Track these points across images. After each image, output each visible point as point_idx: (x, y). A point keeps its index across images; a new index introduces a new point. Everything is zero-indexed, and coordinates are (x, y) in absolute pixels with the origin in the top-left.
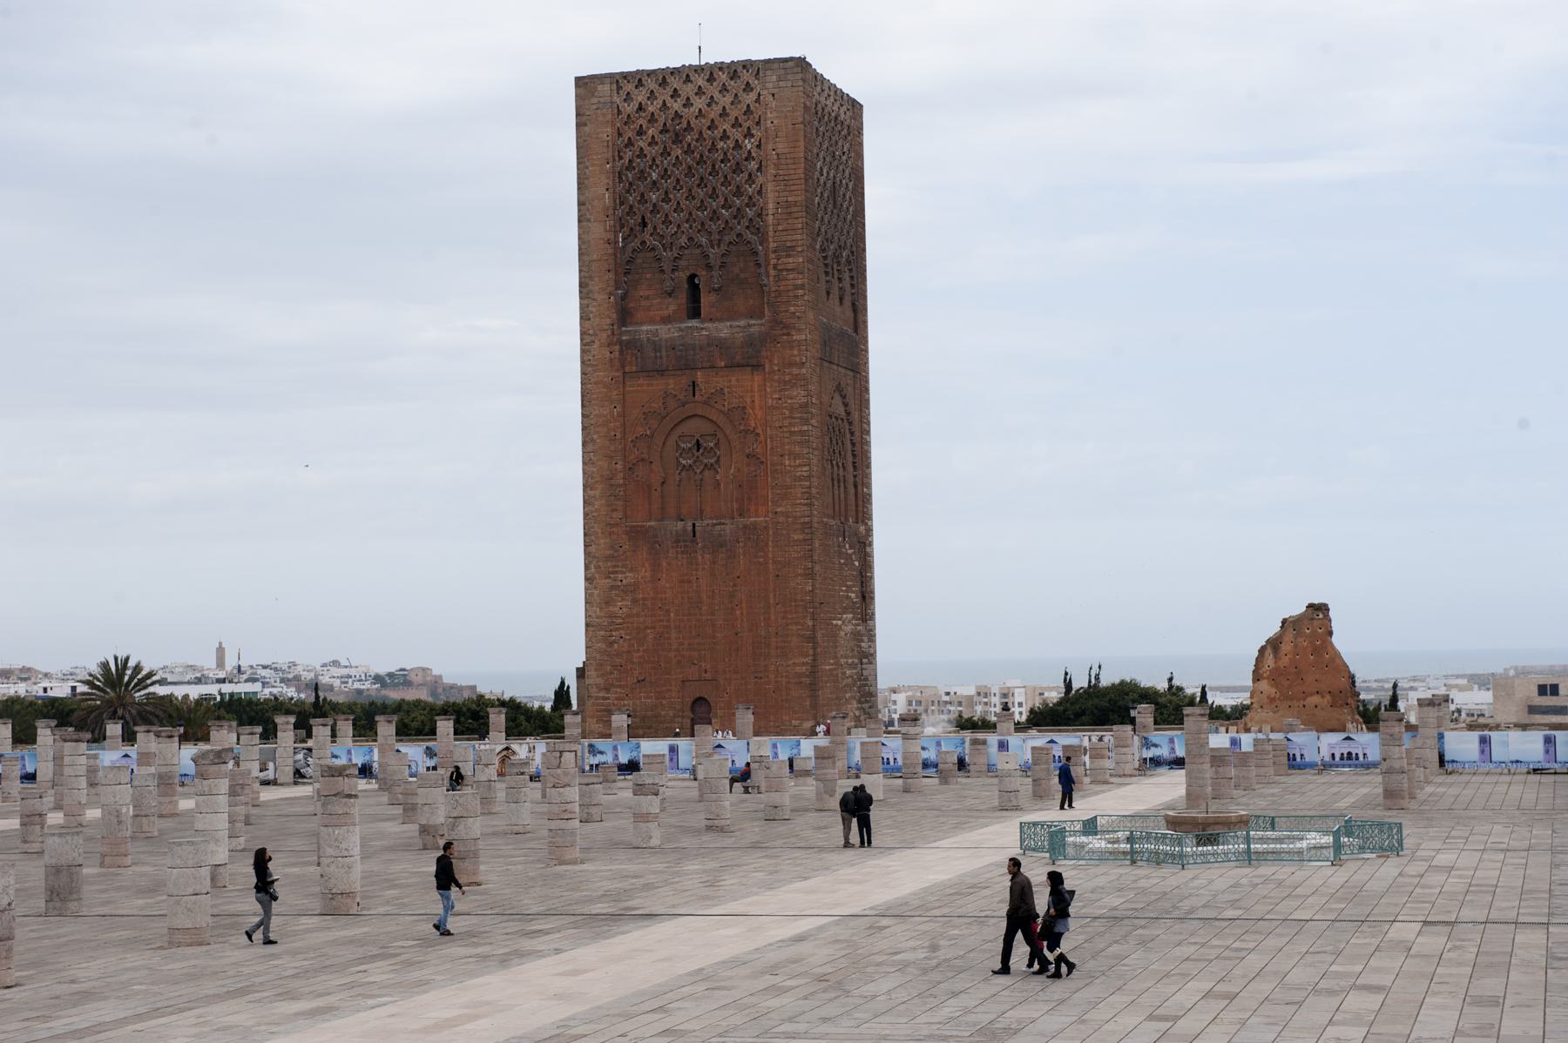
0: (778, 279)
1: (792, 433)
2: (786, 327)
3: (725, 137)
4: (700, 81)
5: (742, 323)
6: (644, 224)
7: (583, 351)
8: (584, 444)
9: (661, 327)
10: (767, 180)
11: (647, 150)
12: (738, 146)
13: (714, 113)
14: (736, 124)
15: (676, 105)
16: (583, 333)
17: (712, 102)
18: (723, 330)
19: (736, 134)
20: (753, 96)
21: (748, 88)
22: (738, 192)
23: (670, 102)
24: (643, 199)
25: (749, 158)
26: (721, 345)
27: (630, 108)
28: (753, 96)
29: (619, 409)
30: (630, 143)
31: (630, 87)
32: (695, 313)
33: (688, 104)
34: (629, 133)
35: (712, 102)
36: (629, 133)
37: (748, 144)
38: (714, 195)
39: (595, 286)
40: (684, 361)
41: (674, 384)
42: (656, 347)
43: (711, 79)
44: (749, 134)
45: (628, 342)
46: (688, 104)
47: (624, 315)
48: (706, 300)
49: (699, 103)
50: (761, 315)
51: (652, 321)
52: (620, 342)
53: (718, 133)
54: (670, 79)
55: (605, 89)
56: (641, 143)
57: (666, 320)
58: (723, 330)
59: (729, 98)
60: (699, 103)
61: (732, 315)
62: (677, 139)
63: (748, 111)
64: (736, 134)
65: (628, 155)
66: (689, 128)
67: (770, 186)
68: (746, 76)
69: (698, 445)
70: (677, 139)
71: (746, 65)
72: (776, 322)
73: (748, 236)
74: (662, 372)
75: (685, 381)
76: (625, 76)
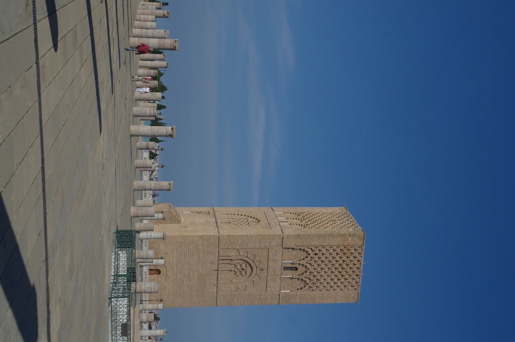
20: (350, 287)
69: (243, 269)
73: (307, 287)
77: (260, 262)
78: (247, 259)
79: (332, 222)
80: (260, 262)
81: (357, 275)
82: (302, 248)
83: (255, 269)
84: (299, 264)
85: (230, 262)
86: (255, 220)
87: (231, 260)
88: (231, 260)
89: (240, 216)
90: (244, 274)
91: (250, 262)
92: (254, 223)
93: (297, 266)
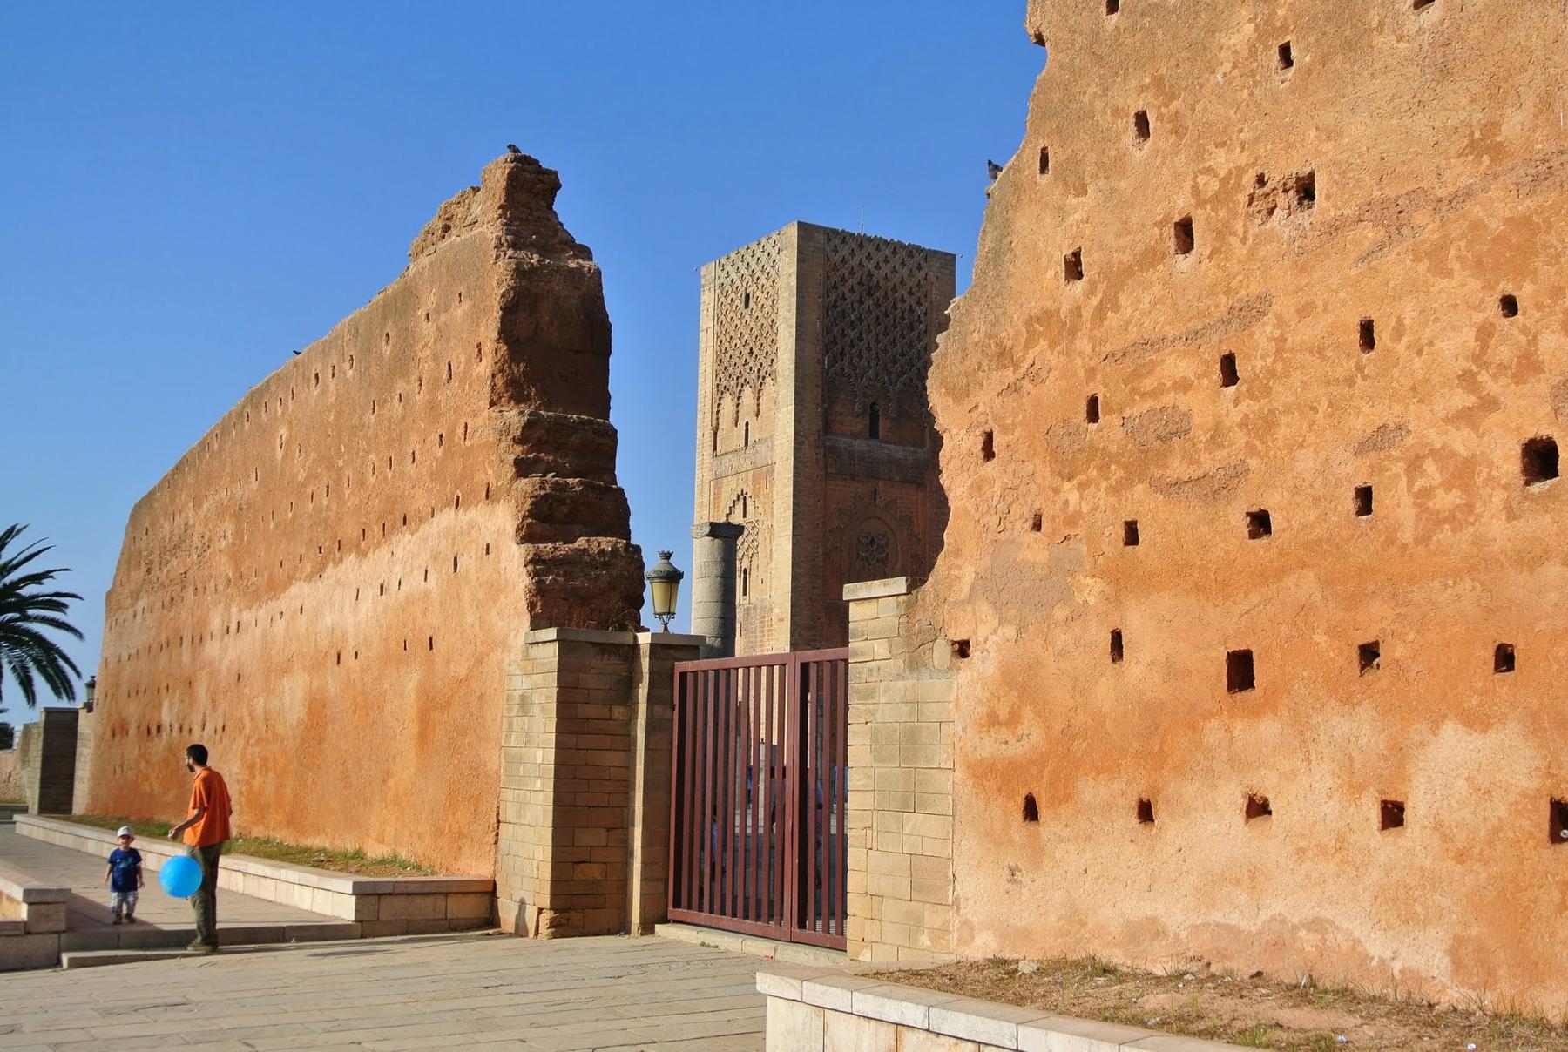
3: (903, 300)
12: (911, 310)
13: (896, 279)
14: (911, 293)
15: (870, 266)
17: (894, 271)
18: (898, 452)
19: (911, 301)
20: (922, 274)
21: (919, 268)
22: (911, 346)
23: (865, 261)
24: (843, 336)
27: (837, 258)
28: (922, 274)
30: (835, 287)
31: (837, 241)
32: (874, 433)
33: (877, 267)
34: (835, 278)
35: (894, 271)
37: (919, 310)
38: (894, 343)
43: (894, 253)
44: (919, 303)
46: (877, 267)
47: (827, 427)
48: (883, 425)
49: (886, 269)
54: (866, 244)
55: (821, 237)
56: (846, 290)
57: (854, 436)
58: (898, 452)
60: (886, 269)
62: (870, 294)
63: (918, 285)
64: (911, 301)
65: (833, 297)
66: (878, 287)
68: (919, 257)
70: (870, 294)
71: (919, 249)
74: (853, 478)
76: (835, 231)
79: (751, 304)
81: (894, 253)
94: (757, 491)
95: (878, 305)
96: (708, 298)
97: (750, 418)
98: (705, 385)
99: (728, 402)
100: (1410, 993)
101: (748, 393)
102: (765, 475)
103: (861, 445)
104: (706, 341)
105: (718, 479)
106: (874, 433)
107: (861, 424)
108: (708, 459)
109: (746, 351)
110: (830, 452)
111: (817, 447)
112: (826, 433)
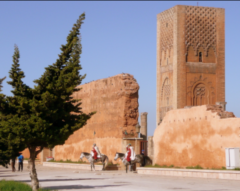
0: (219, 55)
1: (221, 89)
2: (221, 65)
4: (204, 10)
5: (211, 64)
6: (191, 40)
7: (178, 67)
8: (178, 87)
9: (194, 63)
10: (217, 33)
11: (192, 23)
16: (178, 62)
18: (208, 65)
25: (213, 28)
26: (206, 68)
29: (185, 80)
32: (200, 60)
36: (189, 19)
37: (213, 25)
39: (181, 52)
40: (199, 71)
41: (197, 76)
42: (193, 67)
45: (187, 66)
50: (215, 62)
51: (192, 61)
52: (186, 66)
53: (207, 22)
57: (195, 61)
58: (208, 65)
59: (209, 15)
61: (208, 62)
67: (217, 35)
69: (200, 90)
72: (218, 64)
75: (199, 75)
77: (195, 78)
78: (193, 87)
80: (195, 78)
82: (186, 49)
83: (200, 82)
84: (198, 51)
85: (195, 99)
86: (166, 81)
87: (194, 98)
88: (194, 98)
89: (164, 91)
90: (203, 89)
91: (195, 85)
92: (168, 81)
93: (199, 52)
94: (170, 77)
95: (201, 25)
96: (158, 23)
97: (168, 57)
98: (158, 48)
99: (163, 53)
100: (79, 148)
101: (167, 52)
102: (171, 73)
103: (196, 64)
104: (158, 35)
105: (161, 73)
106: (200, 60)
107: (197, 58)
108: (159, 68)
109: (167, 39)
110: (188, 67)
111: (183, 66)
112: (187, 61)
